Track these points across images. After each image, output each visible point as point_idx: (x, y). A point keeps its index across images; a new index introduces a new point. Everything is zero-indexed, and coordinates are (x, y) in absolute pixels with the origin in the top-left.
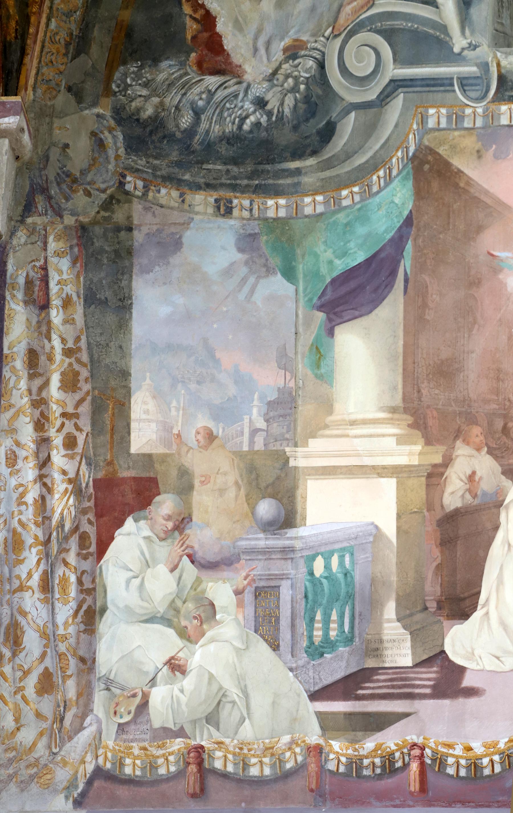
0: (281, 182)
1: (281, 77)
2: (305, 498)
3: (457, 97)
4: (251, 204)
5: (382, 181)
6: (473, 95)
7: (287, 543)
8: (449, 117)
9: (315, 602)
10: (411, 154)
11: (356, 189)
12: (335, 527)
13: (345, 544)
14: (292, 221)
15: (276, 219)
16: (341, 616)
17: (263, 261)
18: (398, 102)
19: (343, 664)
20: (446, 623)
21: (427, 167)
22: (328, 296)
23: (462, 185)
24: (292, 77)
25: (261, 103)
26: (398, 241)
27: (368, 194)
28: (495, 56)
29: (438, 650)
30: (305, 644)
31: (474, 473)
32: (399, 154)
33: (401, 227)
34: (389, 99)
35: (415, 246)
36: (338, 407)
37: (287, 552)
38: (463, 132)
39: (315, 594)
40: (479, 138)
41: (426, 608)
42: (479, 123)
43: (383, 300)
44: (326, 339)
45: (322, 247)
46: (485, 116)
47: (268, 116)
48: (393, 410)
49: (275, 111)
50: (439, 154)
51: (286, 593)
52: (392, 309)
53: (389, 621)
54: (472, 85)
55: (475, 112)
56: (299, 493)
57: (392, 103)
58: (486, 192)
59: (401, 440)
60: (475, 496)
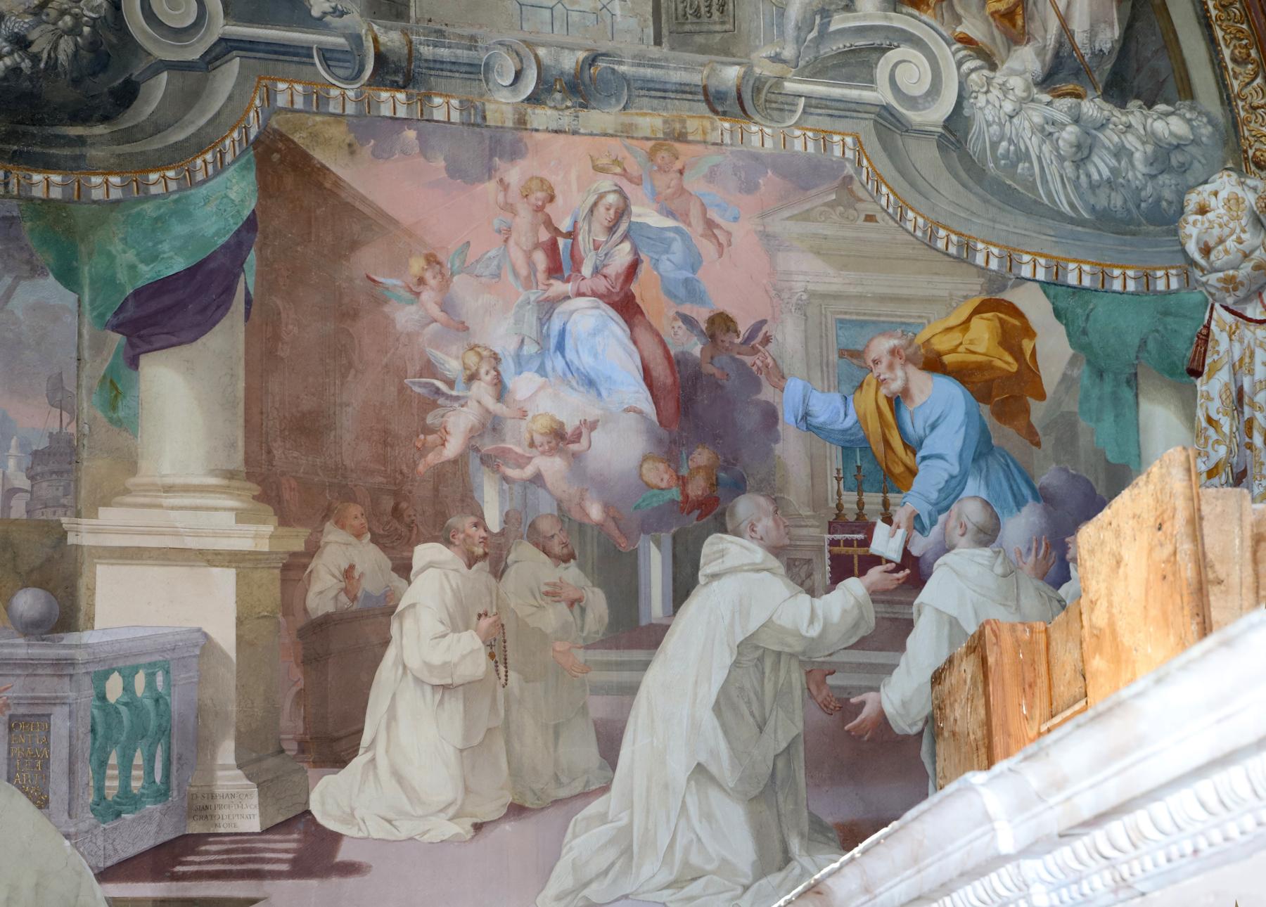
0: (53, 151)
1: (53, 13)
2: (92, 590)
3: (318, 73)
4: (6, 177)
5: (210, 168)
6: (340, 72)
7: (63, 653)
8: (307, 97)
9: (107, 738)
10: (252, 137)
11: (171, 174)
12: (141, 633)
13: (156, 658)
14: (72, 206)
15: (47, 201)
16: (150, 760)
17: (26, 256)
18: (234, 66)
19: (153, 828)
20: (312, 772)
21: (276, 157)
22: (131, 311)
23: (328, 185)
24: (70, 14)
25: (21, 42)
26: (236, 249)
27: (188, 181)
28: (370, 29)
29: (300, 810)
30: (91, 798)
31: (352, 567)
32: (235, 135)
33: (239, 231)
34: (218, 63)
35: (261, 258)
36: (144, 464)
37: (62, 667)
38: (327, 118)
39: (108, 727)
40: (352, 128)
41: (282, 751)
42: (350, 109)
43: (214, 325)
44: (126, 371)
45: (120, 247)
46: (358, 101)
47: (32, 61)
48: (231, 475)
49: (45, 56)
50: (293, 142)
51: (60, 724)
52: (227, 339)
53: (225, 767)
54: (339, 60)
55: (344, 95)
56: (83, 582)
57: (223, 68)
58: (363, 199)
59: (242, 517)
60: (354, 599)
